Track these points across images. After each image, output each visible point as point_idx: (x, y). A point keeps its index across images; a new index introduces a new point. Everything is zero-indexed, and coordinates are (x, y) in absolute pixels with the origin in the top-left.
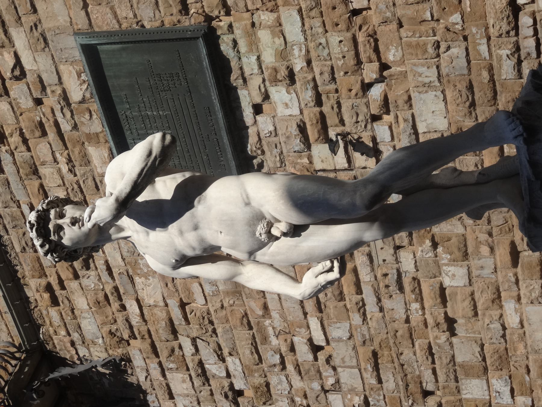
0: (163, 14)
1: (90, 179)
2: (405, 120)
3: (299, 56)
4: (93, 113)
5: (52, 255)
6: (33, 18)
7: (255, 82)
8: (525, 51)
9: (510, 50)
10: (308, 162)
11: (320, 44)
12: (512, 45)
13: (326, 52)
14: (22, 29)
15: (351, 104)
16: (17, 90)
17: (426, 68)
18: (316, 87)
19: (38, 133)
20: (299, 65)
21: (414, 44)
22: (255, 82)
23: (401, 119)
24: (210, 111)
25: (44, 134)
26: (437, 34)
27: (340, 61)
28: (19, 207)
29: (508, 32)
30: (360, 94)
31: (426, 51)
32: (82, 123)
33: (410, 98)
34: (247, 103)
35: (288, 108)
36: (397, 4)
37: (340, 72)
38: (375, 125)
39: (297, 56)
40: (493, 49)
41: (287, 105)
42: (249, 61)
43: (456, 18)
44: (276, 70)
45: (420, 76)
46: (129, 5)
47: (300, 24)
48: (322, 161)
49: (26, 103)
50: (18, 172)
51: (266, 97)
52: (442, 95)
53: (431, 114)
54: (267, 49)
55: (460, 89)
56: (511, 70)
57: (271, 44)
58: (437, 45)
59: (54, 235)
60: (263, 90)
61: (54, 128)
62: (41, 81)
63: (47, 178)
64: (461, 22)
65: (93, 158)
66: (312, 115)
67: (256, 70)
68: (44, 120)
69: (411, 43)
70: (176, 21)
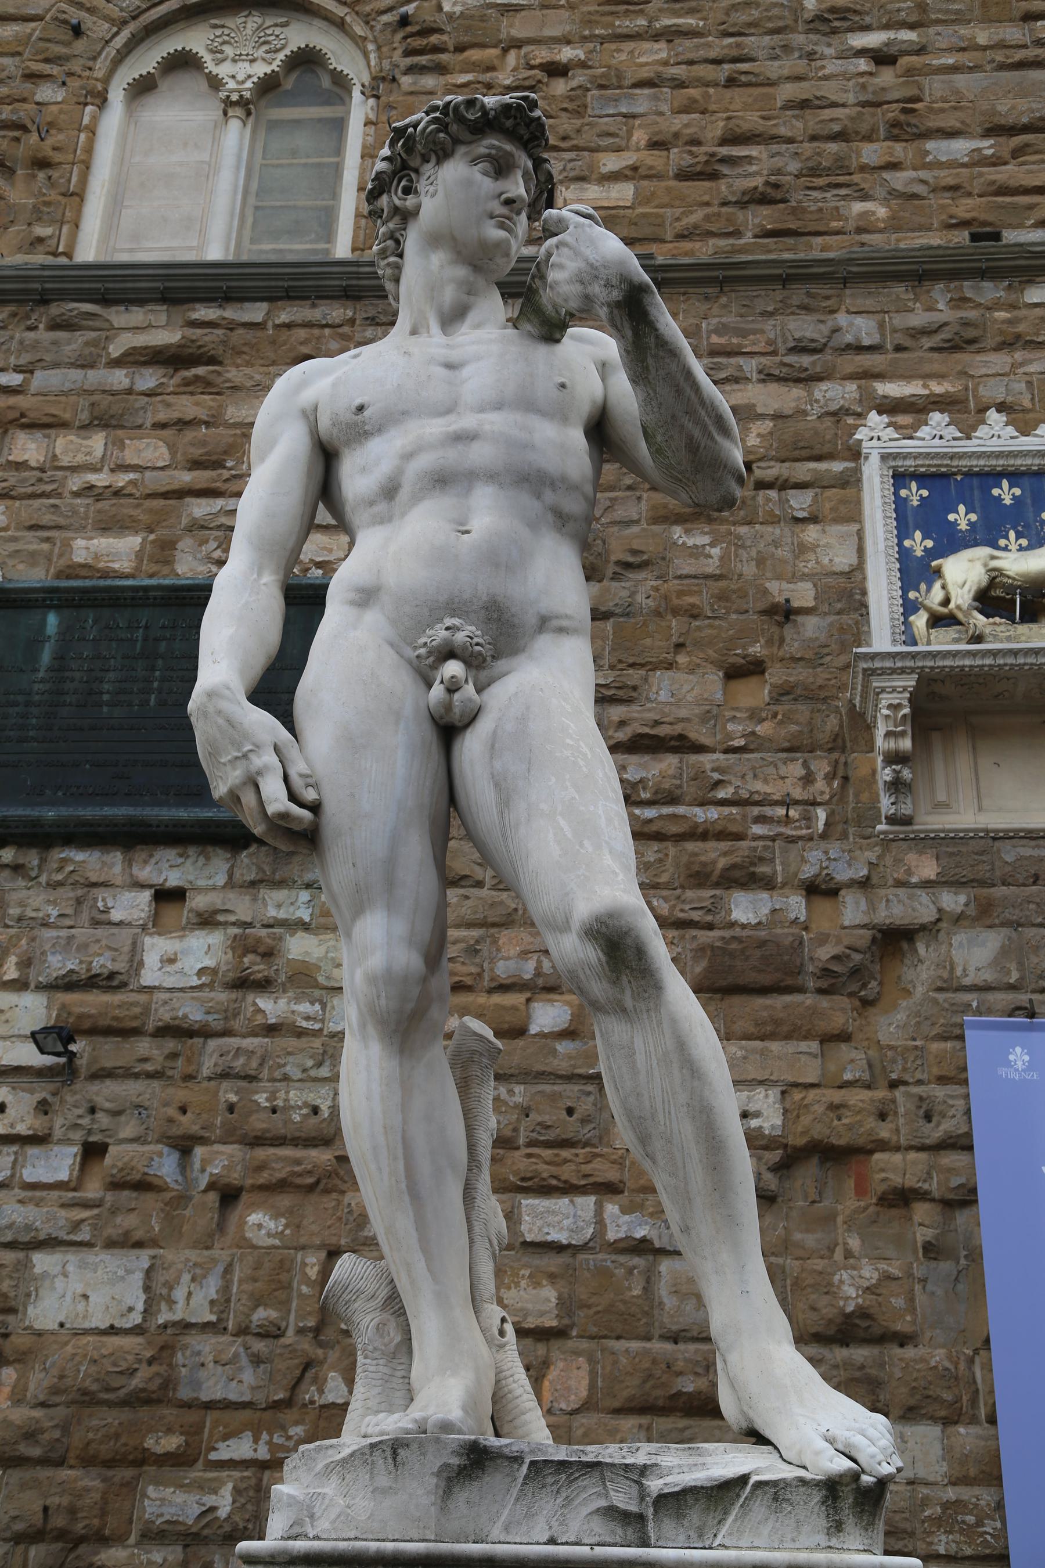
1: (62, 521)
2: (76, 1226)
3: (293, 1012)
5: (435, 120)
7: (242, 907)
8: (217, 1558)
9: (229, 1517)
10: (6, 978)
11: (319, 1065)
13: (297, 1074)
15: (147, 1104)
17: (215, 1297)
18: (205, 1033)
19: (197, 452)
20: (272, 1007)
21: (284, 1277)
22: (242, 907)
27: (267, 1100)
31: (258, 1301)
32: (207, 542)
33: (139, 1245)
34: (191, 878)
35: (161, 961)
37: (237, 1093)
38: (75, 1149)
39: (296, 1007)
40: (236, 1474)
41: (172, 961)
42: (299, 903)
45: (193, 1280)
50: (104, 392)
52: (129, 1325)
53: (80, 1291)
55: (139, 1374)
56: (169, 1513)
57: (333, 959)
58: (272, 1333)
59: (493, 147)
60: (221, 918)
63: (79, 441)
64: (322, 1402)
65: (111, 540)
66: (137, 1010)
67: (272, 912)
68: (226, 474)
69: (288, 1271)
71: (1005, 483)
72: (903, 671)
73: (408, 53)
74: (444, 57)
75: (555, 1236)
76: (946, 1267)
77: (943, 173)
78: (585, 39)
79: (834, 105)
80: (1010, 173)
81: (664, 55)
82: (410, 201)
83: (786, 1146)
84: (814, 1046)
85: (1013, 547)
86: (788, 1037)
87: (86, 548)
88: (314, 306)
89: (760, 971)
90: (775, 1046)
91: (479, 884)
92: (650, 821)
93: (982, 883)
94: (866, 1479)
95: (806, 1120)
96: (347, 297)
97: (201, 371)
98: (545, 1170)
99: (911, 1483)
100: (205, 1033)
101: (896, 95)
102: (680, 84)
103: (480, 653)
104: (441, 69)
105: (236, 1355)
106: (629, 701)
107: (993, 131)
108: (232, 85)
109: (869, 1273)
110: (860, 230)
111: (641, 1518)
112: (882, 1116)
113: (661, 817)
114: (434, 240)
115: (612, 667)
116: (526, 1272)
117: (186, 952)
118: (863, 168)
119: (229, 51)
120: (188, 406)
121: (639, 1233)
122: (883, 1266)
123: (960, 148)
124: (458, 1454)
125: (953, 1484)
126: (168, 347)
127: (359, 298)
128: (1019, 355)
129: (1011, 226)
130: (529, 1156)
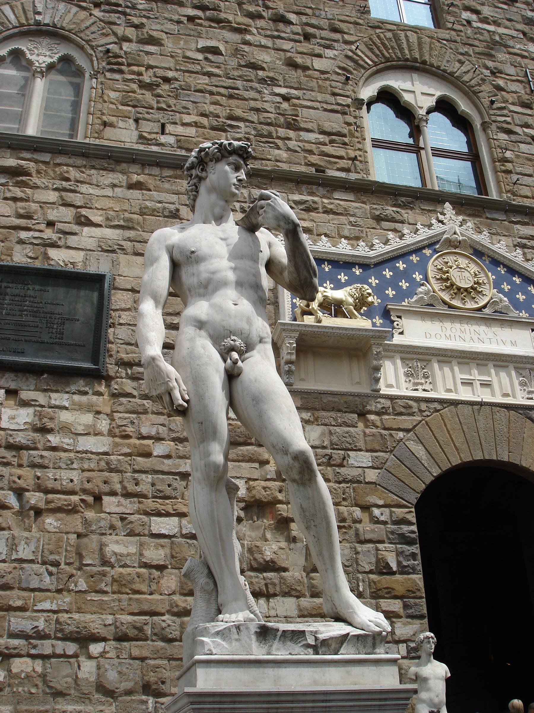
0: (119, 345)
4: (32, 261)
5: (217, 148)
6: (129, 250)
9: (43, 630)
11: (72, 463)
12: (48, 632)
13: (64, 466)
16: (68, 214)
18: (27, 448)
19: (22, 211)
20: (54, 439)
21: (61, 544)
24: (22, 353)
25: (20, 216)
26: (67, 566)
29: (62, 630)
30: (14, 486)
31: (51, 553)
32: (26, 248)
36: (103, 537)
39: (63, 440)
40: (45, 614)
43: (83, 585)
44: (51, 419)
46: (131, 323)
47: (94, 451)
49: (53, 215)
51: (25, 404)
54: (74, 418)
55: (5, 578)
58: (56, 564)
59: (236, 160)
60: (33, 403)
61: (25, 225)
67: (53, 402)
68: (34, 222)
70: (112, 353)
71: (326, 263)
72: (294, 330)
73: (109, 63)
74: (123, 67)
75: (163, 531)
76: (299, 545)
77: (306, 145)
78: (177, 70)
79: (268, 112)
80: (328, 149)
81: (207, 82)
82: (204, 174)
83: (246, 501)
84: (257, 465)
85: (329, 287)
86: (248, 461)
88: (70, 158)
89: (239, 437)
90: (243, 464)
91: (134, 397)
93: (315, 409)
95: (254, 492)
96: (83, 156)
97: (24, 178)
98: (161, 508)
99: (285, 617)
100: (27, 448)
101: (290, 113)
102: (212, 93)
104: (121, 72)
105: (43, 572)
107: (323, 132)
108: (37, 64)
109: (275, 547)
110: (277, 161)
112: (280, 491)
114: (212, 190)
116: (153, 544)
117: (18, 416)
118: (279, 138)
119: (36, 51)
120: (18, 192)
122: (279, 544)
123: (312, 137)
124: (259, 628)
125: (299, 617)
126: (11, 167)
127: (87, 157)
128: (331, 216)
129: (328, 168)
130: (154, 501)
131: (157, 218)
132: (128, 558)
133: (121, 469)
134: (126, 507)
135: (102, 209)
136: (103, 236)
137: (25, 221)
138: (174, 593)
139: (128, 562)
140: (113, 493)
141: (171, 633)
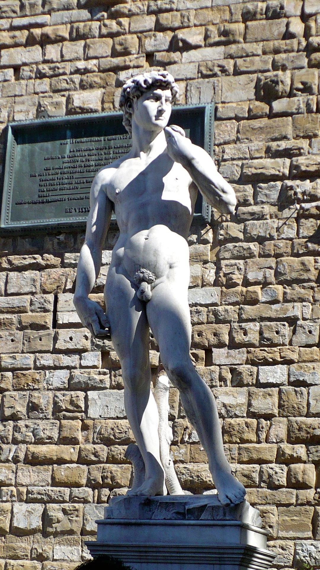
14: (222, 57)
23: (102, 377)
28: (44, 13)
46: (236, 157)
47: (203, 303)
48: (66, 301)
49: (149, 44)
62: (170, 63)
64: (191, 441)
75: (271, 380)
87: (80, 98)
91: (240, 241)
92: (308, 210)
94: (232, 505)
103: (151, 279)
106: (300, 154)
111: (184, 513)
113: (312, 207)
115: (294, 138)
121: (301, 379)
130: (261, 350)
131: (261, 22)
132: (238, 408)
133: (229, 319)
134: (234, 358)
135: (201, 25)
136: (204, 59)
137: (122, 58)
138: (282, 441)
139: (237, 413)
140: (221, 345)
141: (278, 480)
